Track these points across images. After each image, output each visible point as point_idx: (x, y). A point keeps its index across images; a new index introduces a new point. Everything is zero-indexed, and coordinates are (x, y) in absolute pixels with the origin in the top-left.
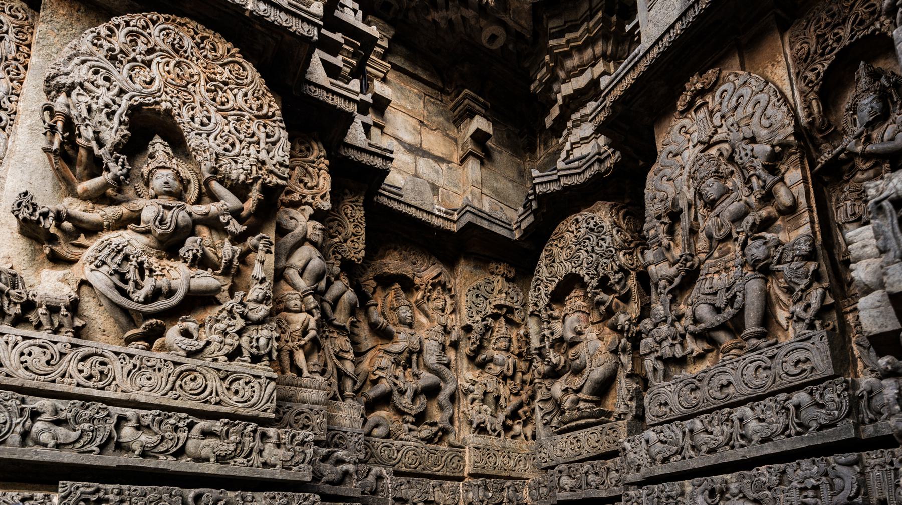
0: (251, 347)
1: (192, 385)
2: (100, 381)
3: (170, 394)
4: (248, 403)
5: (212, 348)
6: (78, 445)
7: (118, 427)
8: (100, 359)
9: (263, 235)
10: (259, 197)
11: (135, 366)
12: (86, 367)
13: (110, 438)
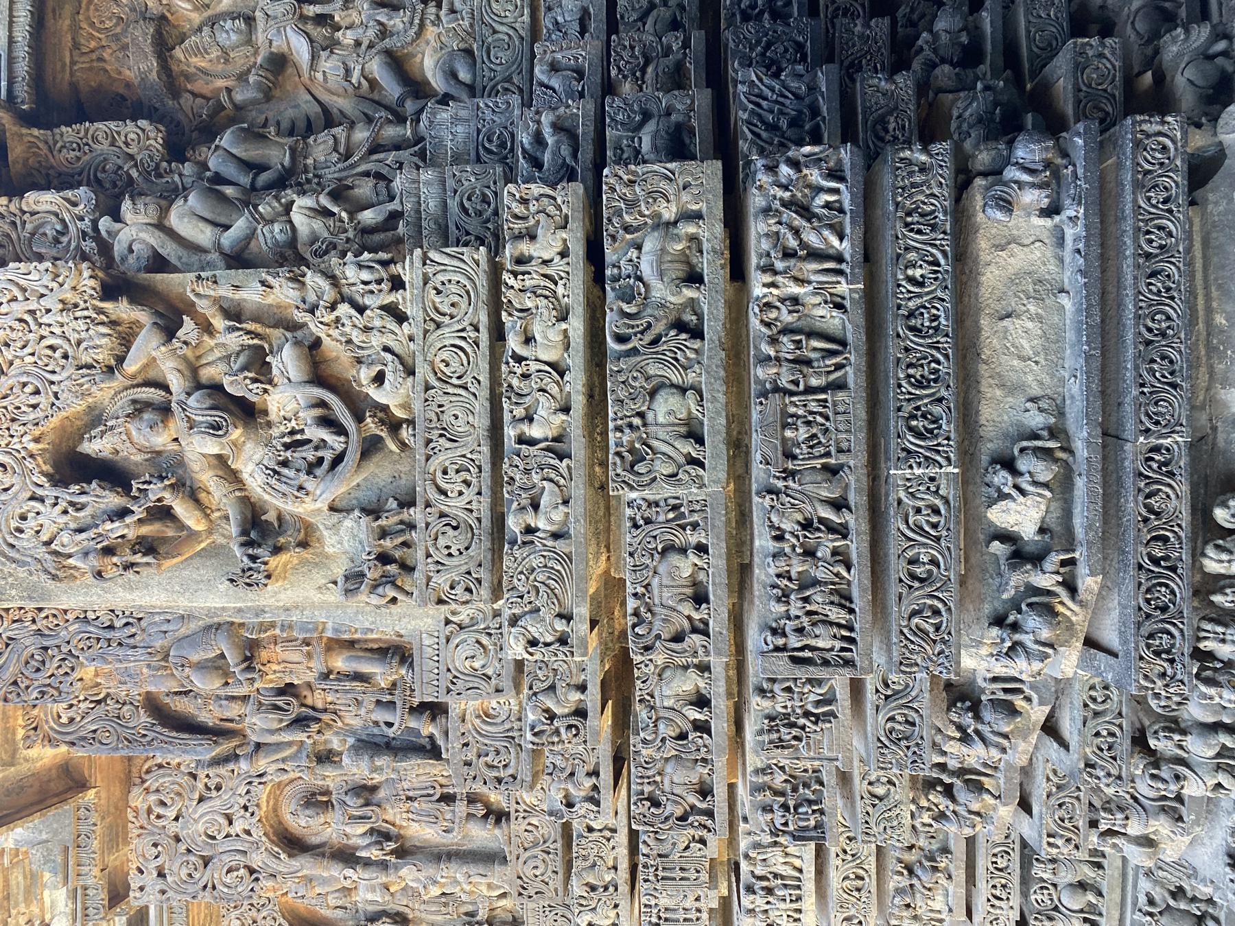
0: (380, 291)
1: (455, 365)
2: (469, 471)
3: (472, 390)
4: (469, 287)
5: (391, 344)
6: (562, 482)
7: (532, 442)
8: (439, 474)
11: (441, 435)
12: (453, 488)
13: (548, 449)
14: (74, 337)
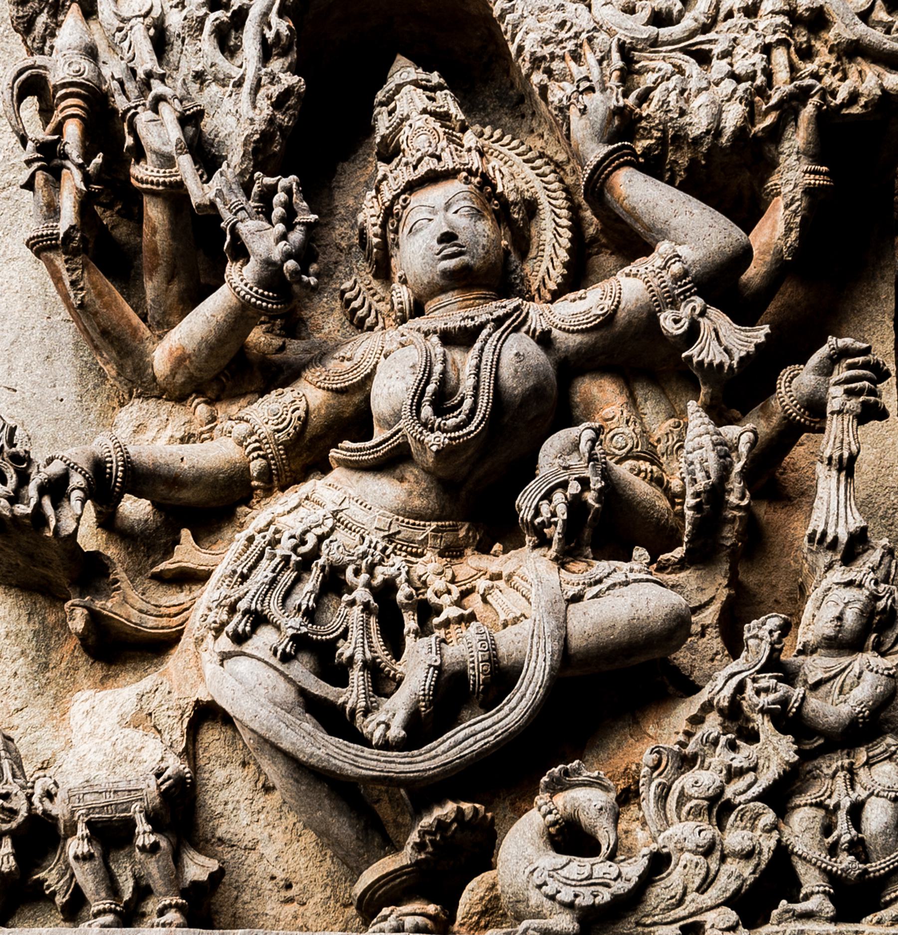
9: (841, 342)
10: (811, 179)
14: (720, 39)
